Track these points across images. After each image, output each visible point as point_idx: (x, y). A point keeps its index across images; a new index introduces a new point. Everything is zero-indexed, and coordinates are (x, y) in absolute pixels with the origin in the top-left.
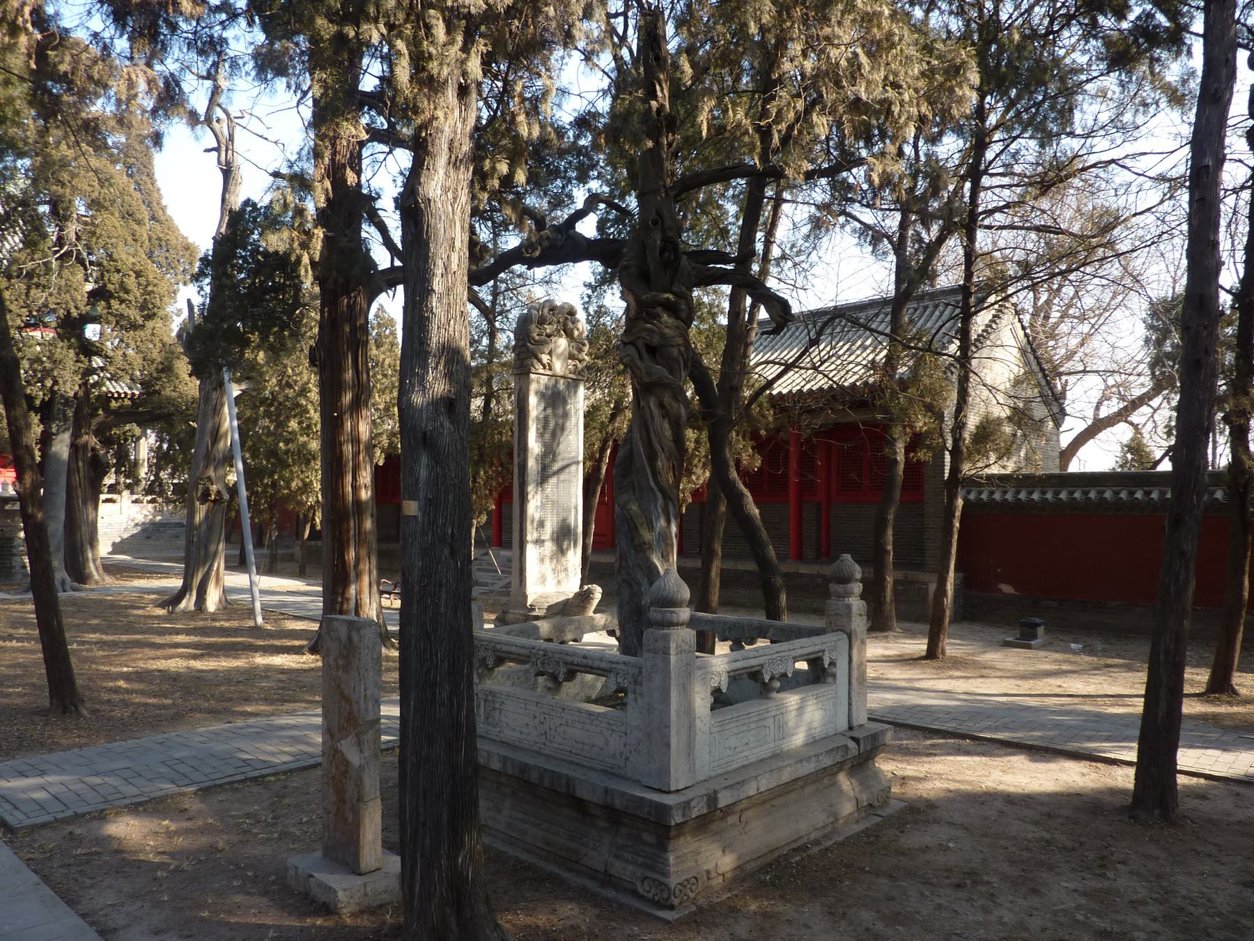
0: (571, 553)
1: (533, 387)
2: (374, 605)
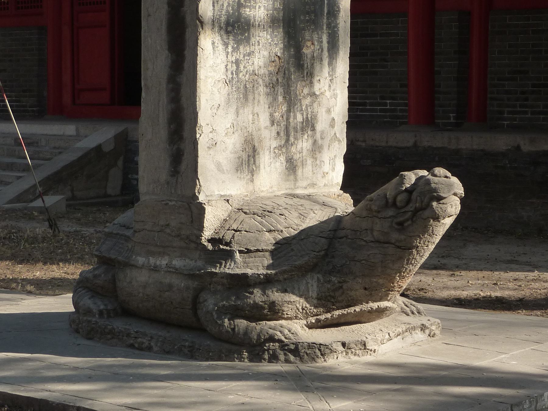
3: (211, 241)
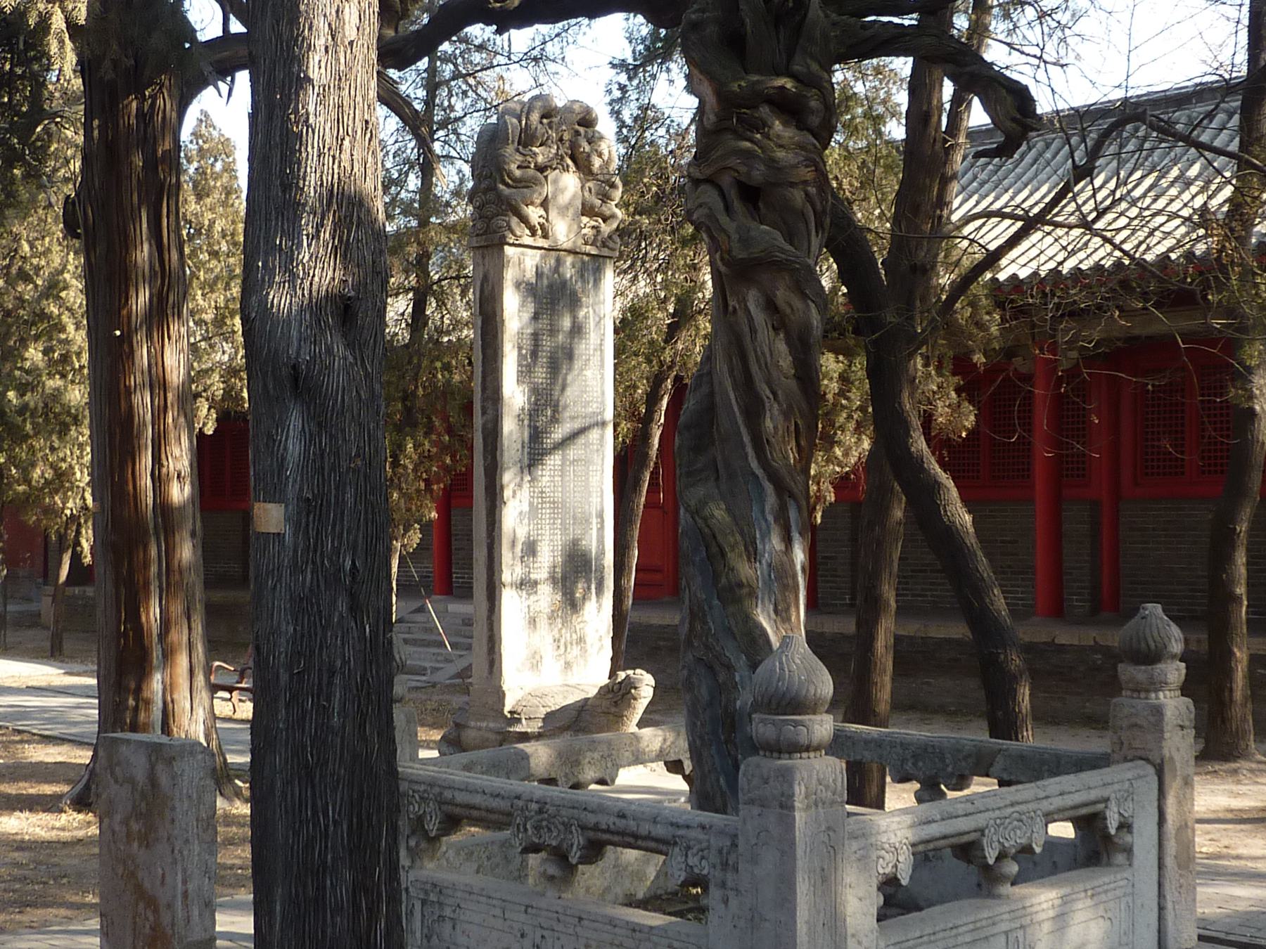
0: (590, 607)
1: (510, 275)
2: (200, 714)
3: (510, 712)
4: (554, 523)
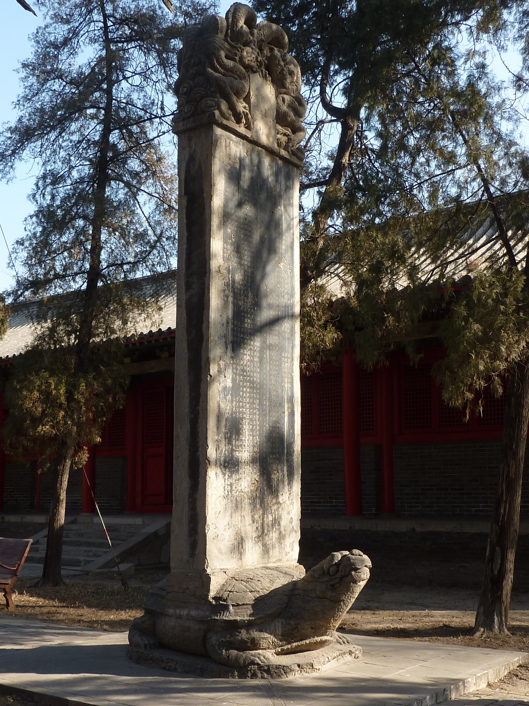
3: (215, 598)
4: (253, 403)
